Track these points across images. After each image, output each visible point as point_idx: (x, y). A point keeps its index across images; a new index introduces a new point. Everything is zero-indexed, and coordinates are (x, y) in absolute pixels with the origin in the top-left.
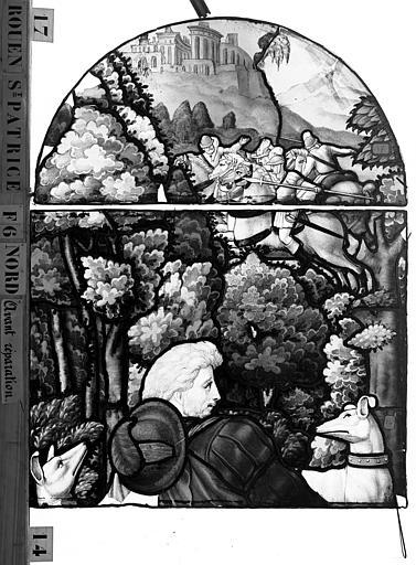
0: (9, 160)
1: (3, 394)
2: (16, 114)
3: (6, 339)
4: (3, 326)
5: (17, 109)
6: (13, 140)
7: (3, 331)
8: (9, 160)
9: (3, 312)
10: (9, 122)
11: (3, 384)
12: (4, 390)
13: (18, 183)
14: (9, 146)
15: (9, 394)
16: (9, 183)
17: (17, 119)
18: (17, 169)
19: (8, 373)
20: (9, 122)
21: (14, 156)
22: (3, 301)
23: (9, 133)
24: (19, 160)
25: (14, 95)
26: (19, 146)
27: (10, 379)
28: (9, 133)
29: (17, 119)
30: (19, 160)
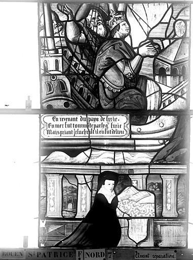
0: (61, 256)
3: (151, 257)
4: (145, 258)
7: (147, 258)
8: (61, 256)
9: (140, 258)
10: (45, 256)
13: (70, 252)
14: (55, 257)
15: (173, 257)
16: (70, 256)
17: (44, 254)
20: (45, 256)
21: (59, 256)
22: (135, 258)
23: (50, 257)
26: (55, 253)
28: (50, 257)
29: (44, 254)
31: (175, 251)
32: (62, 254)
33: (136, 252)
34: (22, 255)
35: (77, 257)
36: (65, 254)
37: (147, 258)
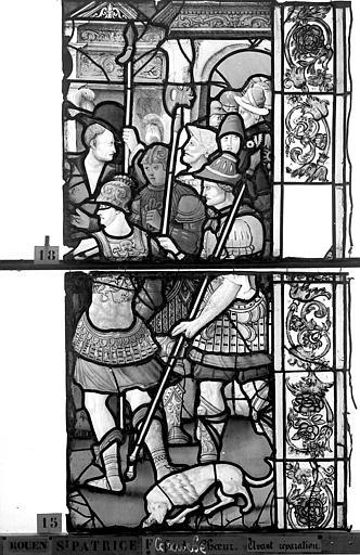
1: (315, 551)
2: (81, 544)
3: (276, 549)
5: (78, 544)
6: (100, 547)
10: (87, 549)
11: (308, 550)
12: (312, 550)
14: (104, 549)
18: (121, 545)
19: (300, 547)
24: (115, 543)
25: (67, 546)
27: (304, 545)
29: (85, 545)
30: (115, 543)
31: (320, 537)
32: (117, 546)
33: (250, 539)
34: (45, 546)
35: (144, 549)
36: (124, 545)
37: (268, 550)
